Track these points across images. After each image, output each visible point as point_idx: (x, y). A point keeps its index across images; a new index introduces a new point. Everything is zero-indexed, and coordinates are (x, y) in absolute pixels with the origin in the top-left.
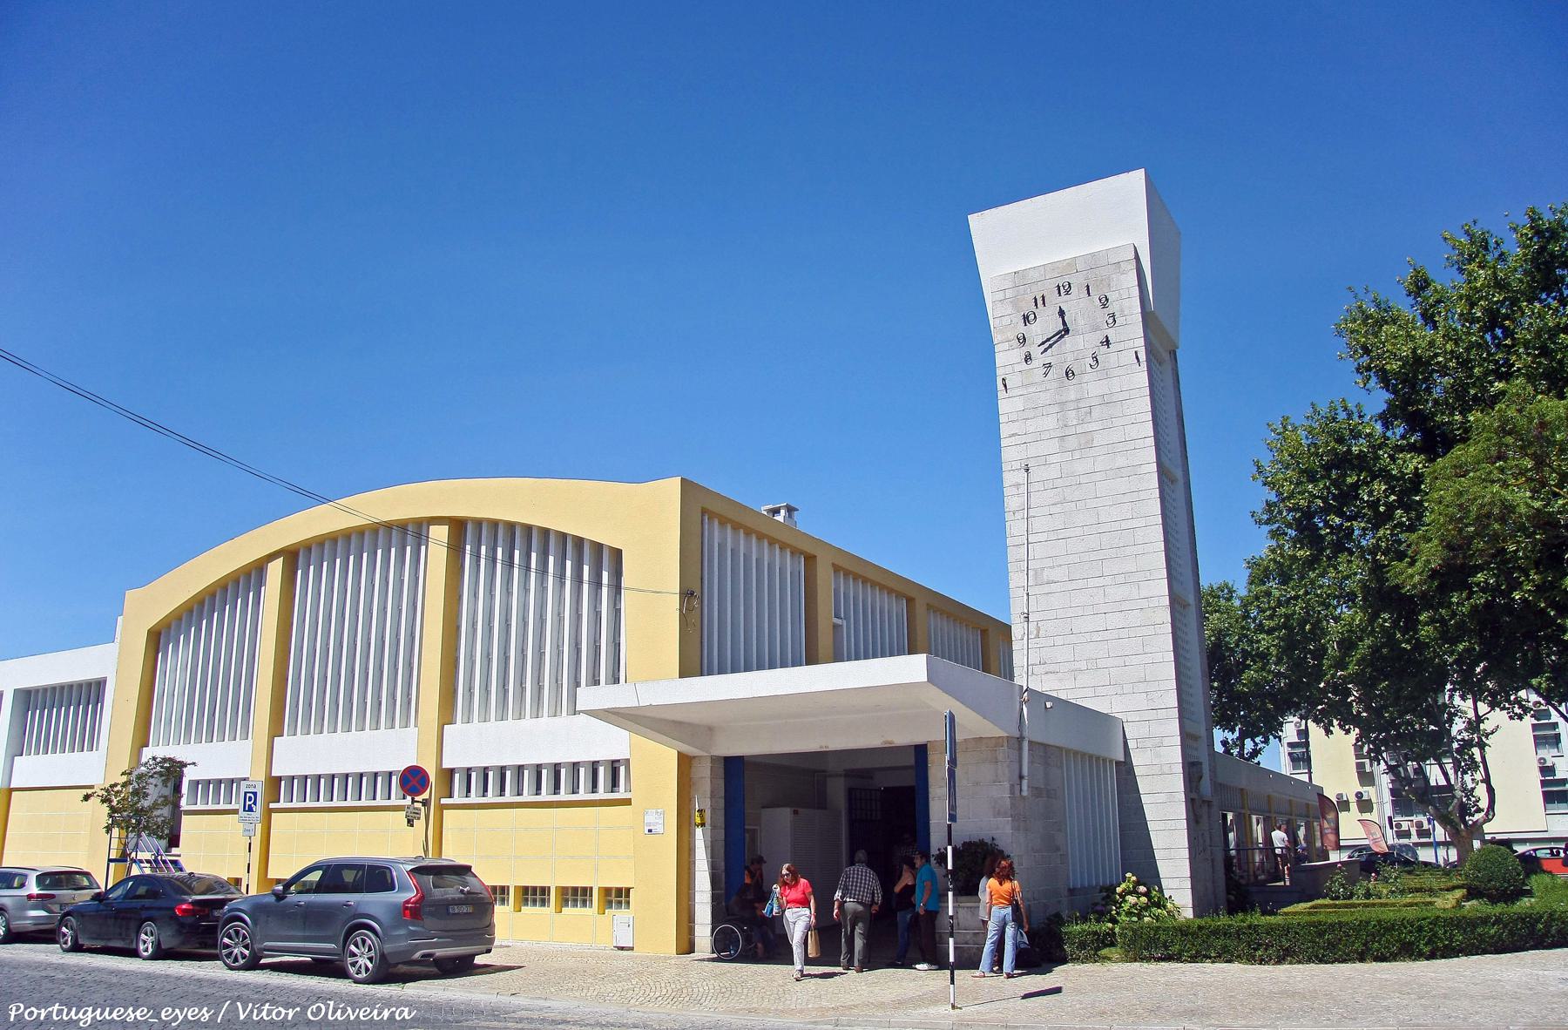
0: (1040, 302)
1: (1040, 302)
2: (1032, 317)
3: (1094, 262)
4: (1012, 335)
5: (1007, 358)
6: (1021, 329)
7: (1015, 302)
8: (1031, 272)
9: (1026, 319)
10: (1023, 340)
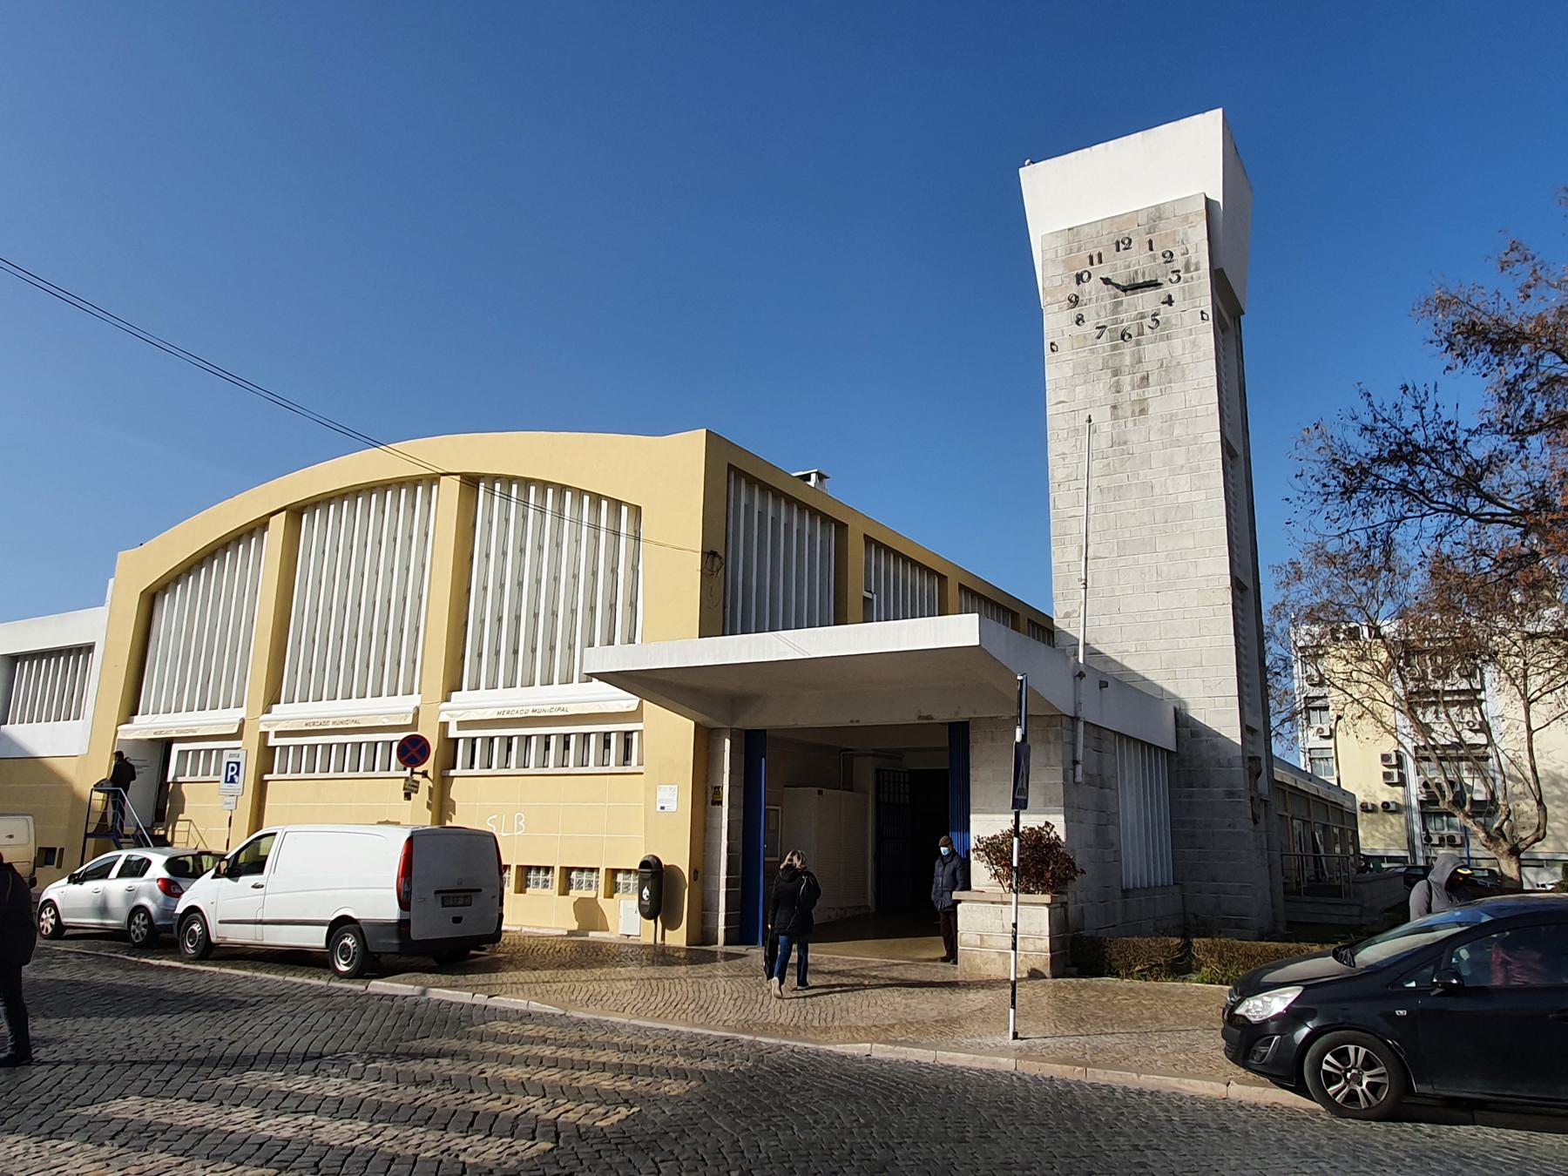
0: (1096, 260)
1: (1096, 260)
2: (1085, 276)
3: (1157, 215)
4: (1063, 296)
5: (1056, 322)
6: (1074, 289)
7: (1067, 263)
8: (1086, 228)
9: (1079, 278)
10: (1075, 301)
